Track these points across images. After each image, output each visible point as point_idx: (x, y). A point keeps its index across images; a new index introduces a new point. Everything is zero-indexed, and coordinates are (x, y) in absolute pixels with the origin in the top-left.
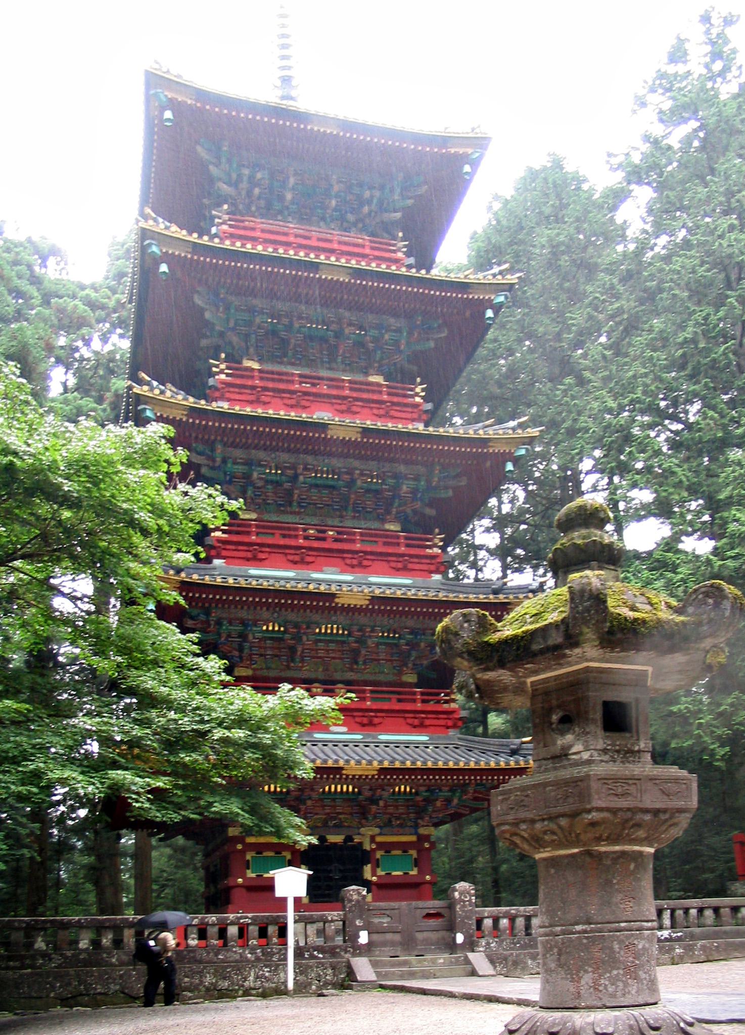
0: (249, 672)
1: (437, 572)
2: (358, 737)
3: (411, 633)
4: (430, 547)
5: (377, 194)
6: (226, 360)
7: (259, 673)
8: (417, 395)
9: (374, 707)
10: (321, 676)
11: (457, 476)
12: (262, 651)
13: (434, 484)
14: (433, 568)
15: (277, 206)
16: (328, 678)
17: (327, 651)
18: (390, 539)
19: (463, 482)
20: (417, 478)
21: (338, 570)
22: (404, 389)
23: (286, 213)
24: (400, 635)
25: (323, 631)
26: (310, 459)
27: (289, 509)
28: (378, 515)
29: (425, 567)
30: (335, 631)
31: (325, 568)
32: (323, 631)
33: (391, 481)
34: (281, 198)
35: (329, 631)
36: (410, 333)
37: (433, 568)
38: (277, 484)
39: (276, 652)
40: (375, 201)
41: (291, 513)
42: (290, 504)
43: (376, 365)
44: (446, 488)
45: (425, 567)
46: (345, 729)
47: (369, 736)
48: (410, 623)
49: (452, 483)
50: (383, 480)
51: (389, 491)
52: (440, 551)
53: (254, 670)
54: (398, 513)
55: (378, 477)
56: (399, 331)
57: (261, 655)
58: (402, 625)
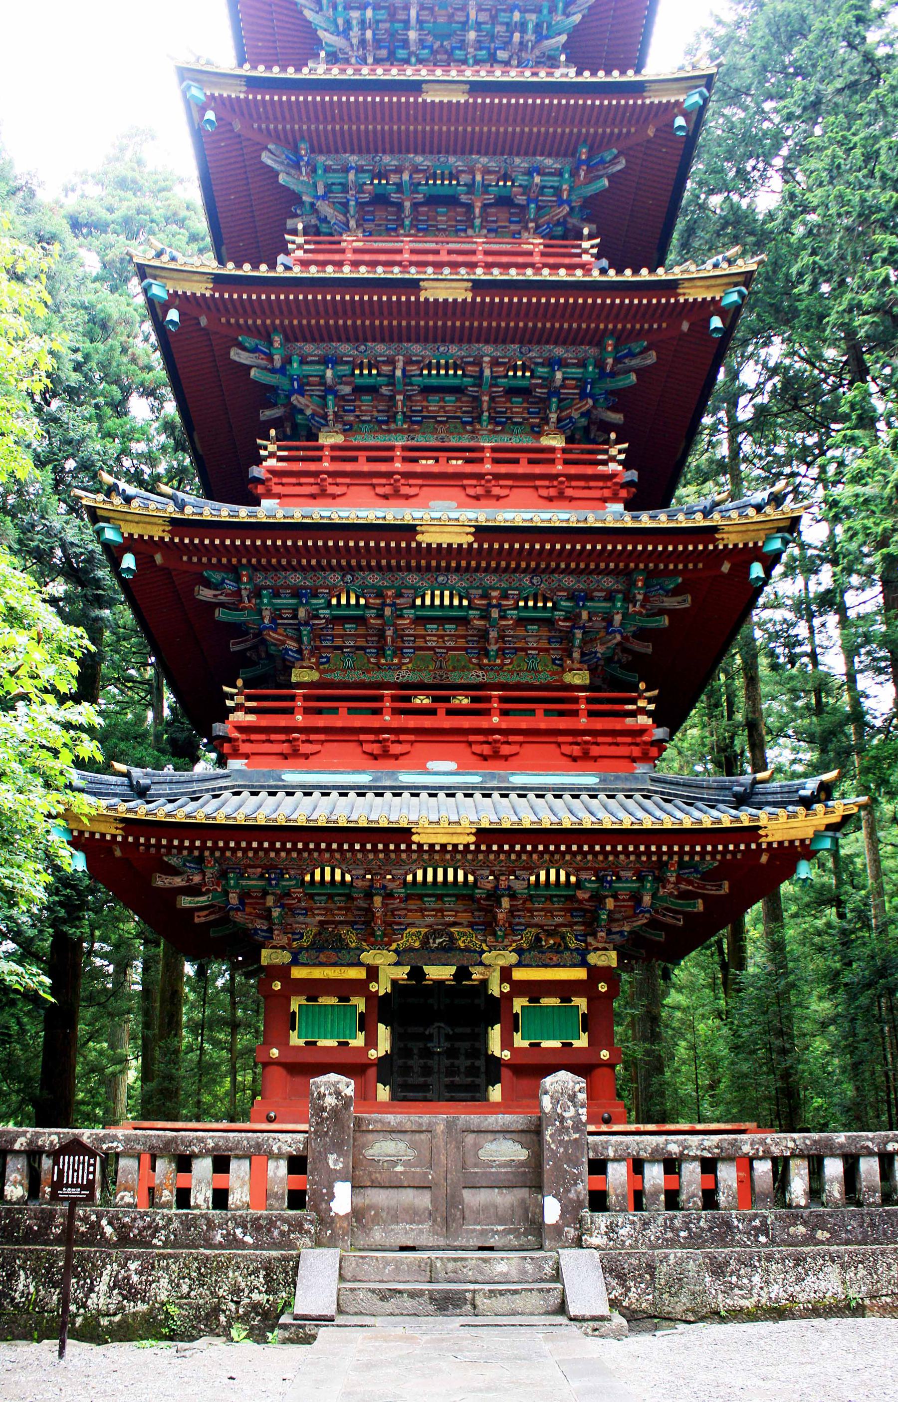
0: (315, 676)
1: (615, 499)
2: (475, 779)
3: (568, 599)
4: (605, 463)
5: (532, 18)
6: (305, 233)
7: (328, 676)
8: (586, 251)
9: (504, 726)
10: (427, 678)
11: (645, 350)
12: (338, 642)
13: (608, 370)
14: (607, 493)
15: (401, 53)
16: (437, 681)
17: (442, 637)
18: (545, 455)
19: (652, 358)
20: (582, 364)
21: (454, 504)
22: (565, 247)
23: (413, 60)
24: (554, 604)
25: (428, 602)
26: (416, 349)
27: (393, 426)
28: (532, 426)
29: (597, 494)
30: (447, 602)
31: (431, 503)
32: (428, 602)
33: (542, 371)
34: (405, 43)
35: (437, 602)
36: (574, 173)
37: (607, 493)
38: (373, 390)
39: (361, 642)
40: (530, 26)
41: (397, 431)
42: (392, 418)
43: (531, 225)
44: (627, 371)
45: (597, 494)
46: (452, 766)
47: (493, 776)
48: (569, 581)
49: (635, 362)
50: (532, 372)
51: (541, 386)
52: (620, 468)
53: (321, 672)
54: (559, 420)
55: (524, 368)
56: (559, 173)
57: (340, 648)
58: (555, 585)
